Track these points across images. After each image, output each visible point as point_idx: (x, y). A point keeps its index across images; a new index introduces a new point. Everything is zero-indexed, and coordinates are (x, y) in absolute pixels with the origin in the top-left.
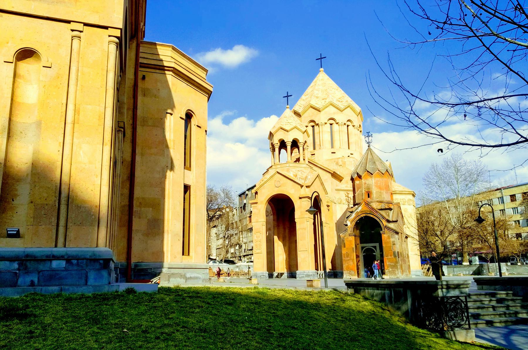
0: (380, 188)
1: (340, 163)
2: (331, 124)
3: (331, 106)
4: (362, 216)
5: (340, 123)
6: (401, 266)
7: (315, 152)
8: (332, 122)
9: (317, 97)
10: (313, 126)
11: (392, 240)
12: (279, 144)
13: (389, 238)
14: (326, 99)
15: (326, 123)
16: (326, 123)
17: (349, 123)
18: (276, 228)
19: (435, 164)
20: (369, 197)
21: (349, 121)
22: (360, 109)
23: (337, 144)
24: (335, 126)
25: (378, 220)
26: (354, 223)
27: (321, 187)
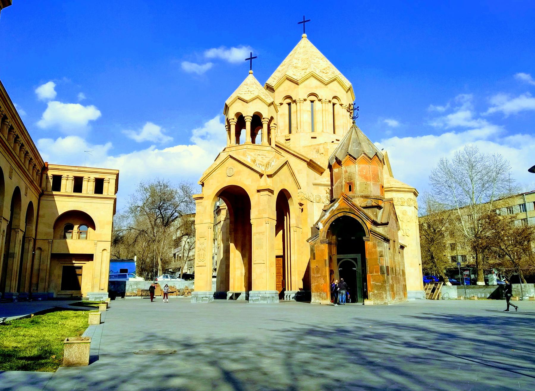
0: (366, 178)
1: (322, 151)
2: (312, 102)
3: (312, 78)
4: (339, 215)
5: (323, 100)
6: (392, 287)
7: (291, 136)
8: (313, 98)
9: (296, 67)
10: (289, 104)
11: (379, 249)
12: (236, 120)
13: (375, 246)
14: (306, 69)
15: (305, 100)
16: (305, 100)
17: (335, 101)
18: (233, 233)
19: (445, 159)
20: (350, 190)
21: (335, 97)
22: (351, 84)
23: (319, 127)
24: (317, 104)
25: (360, 221)
26: (328, 225)
27: (291, 179)
